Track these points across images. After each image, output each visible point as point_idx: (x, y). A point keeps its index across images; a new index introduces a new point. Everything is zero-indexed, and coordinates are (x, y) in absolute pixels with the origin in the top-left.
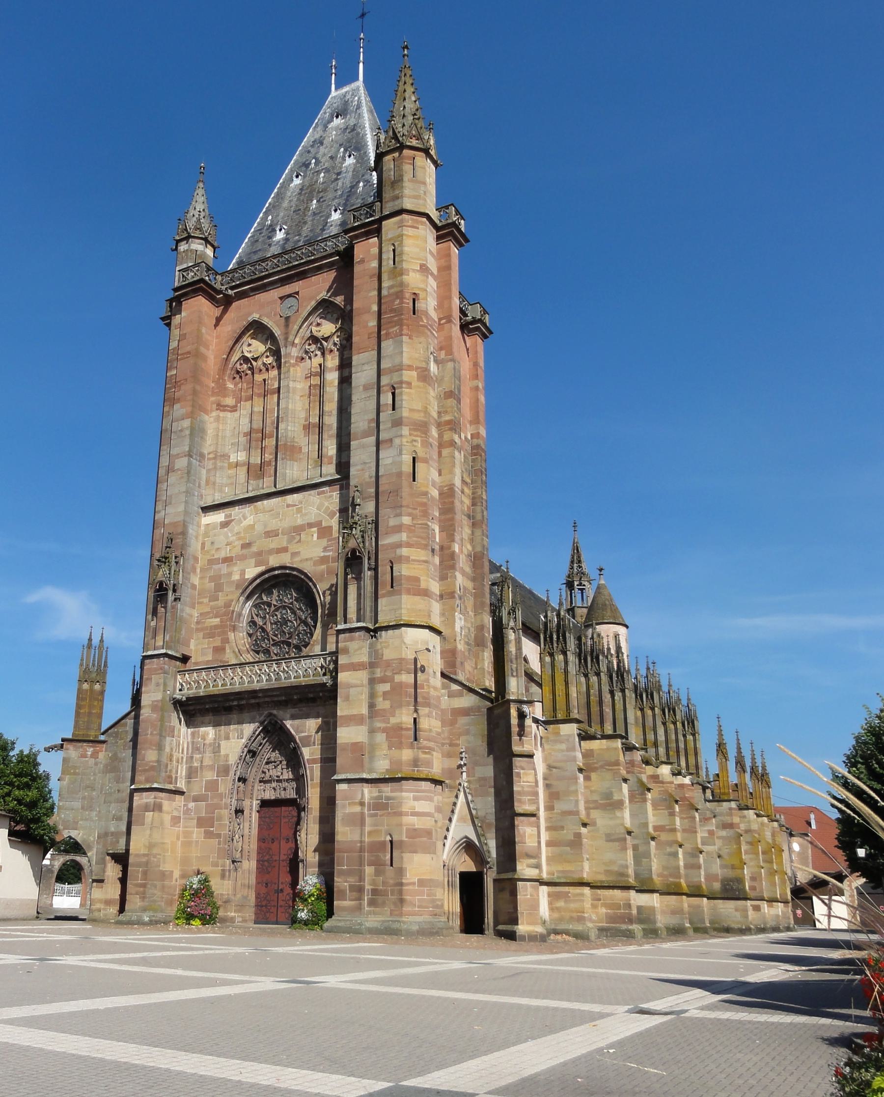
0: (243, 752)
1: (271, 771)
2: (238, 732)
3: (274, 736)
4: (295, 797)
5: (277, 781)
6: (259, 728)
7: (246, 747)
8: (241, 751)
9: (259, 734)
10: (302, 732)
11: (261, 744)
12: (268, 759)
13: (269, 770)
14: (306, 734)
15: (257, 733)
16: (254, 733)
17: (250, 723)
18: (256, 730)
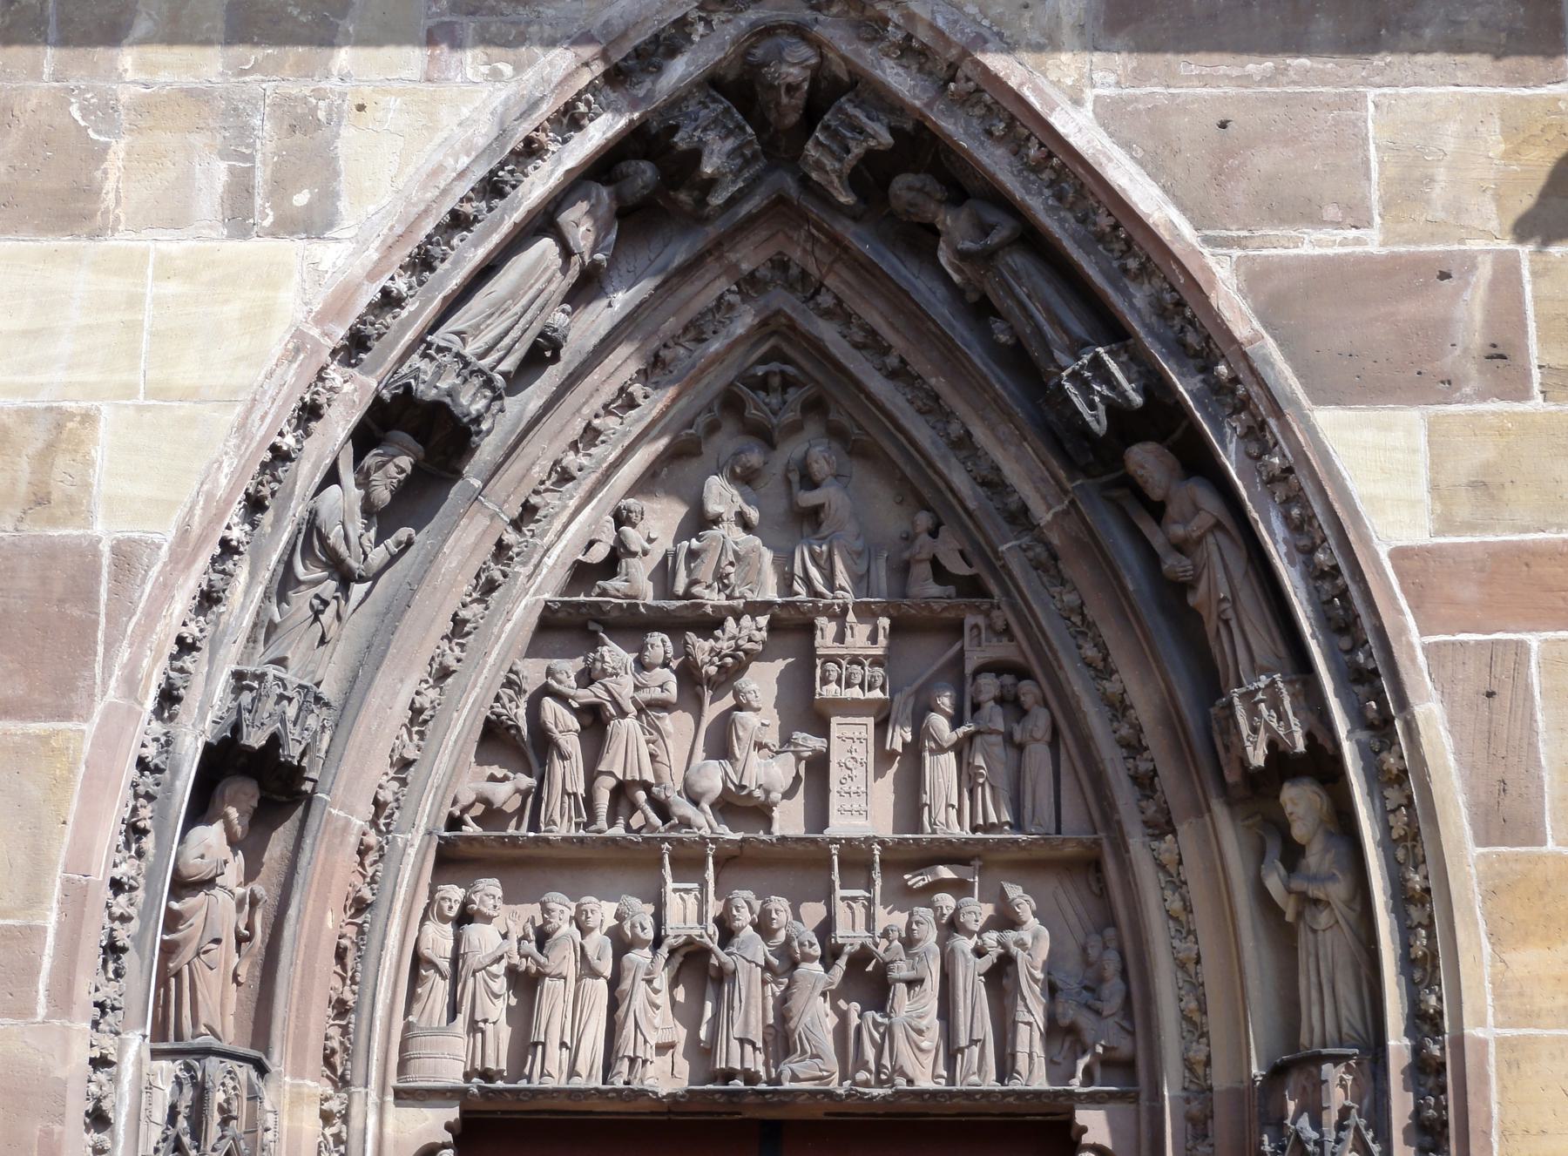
0: (310, 413)
1: (626, 730)
2: (238, 149)
3: (712, 287)
4: (1034, 1075)
5: (733, 861)
6: (570, 120)
7: (356, 346)
8: (292, 386)
9: (543, 222)
10: (1309, 215)
11: (542, 352)
12: (582, 574)
13: (594, 722)
14: (1372, 242)
15: (538, 184)
16: (492, 188)
17: (439, 35)
18: (531, 150)
